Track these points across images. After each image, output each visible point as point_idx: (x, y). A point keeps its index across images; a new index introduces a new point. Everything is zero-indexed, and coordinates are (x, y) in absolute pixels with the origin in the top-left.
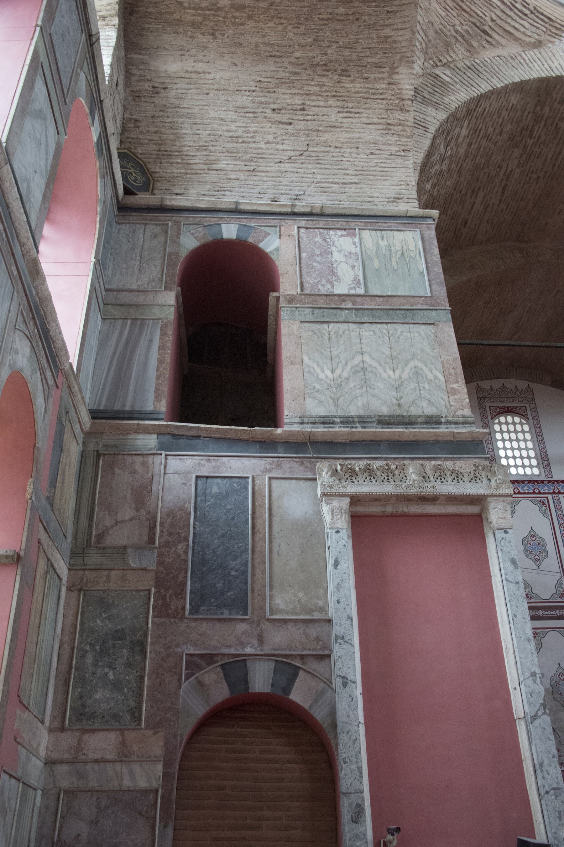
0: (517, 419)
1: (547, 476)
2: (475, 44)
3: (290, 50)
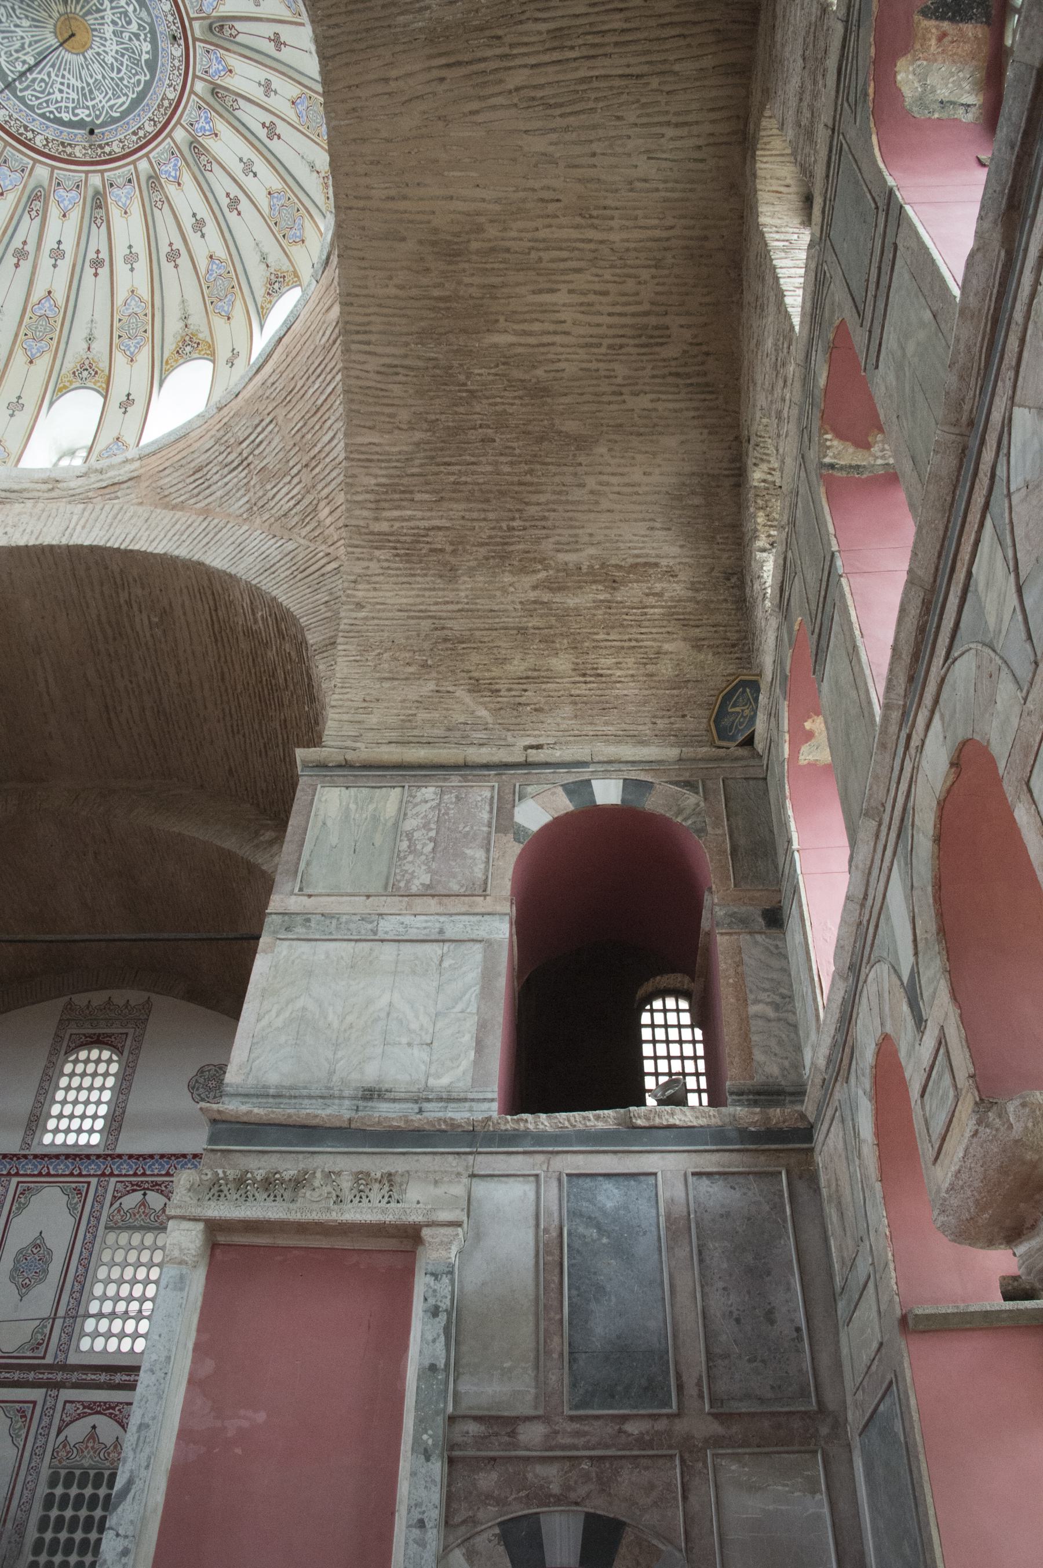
0: (106, 1054)
1: (106, 1147)
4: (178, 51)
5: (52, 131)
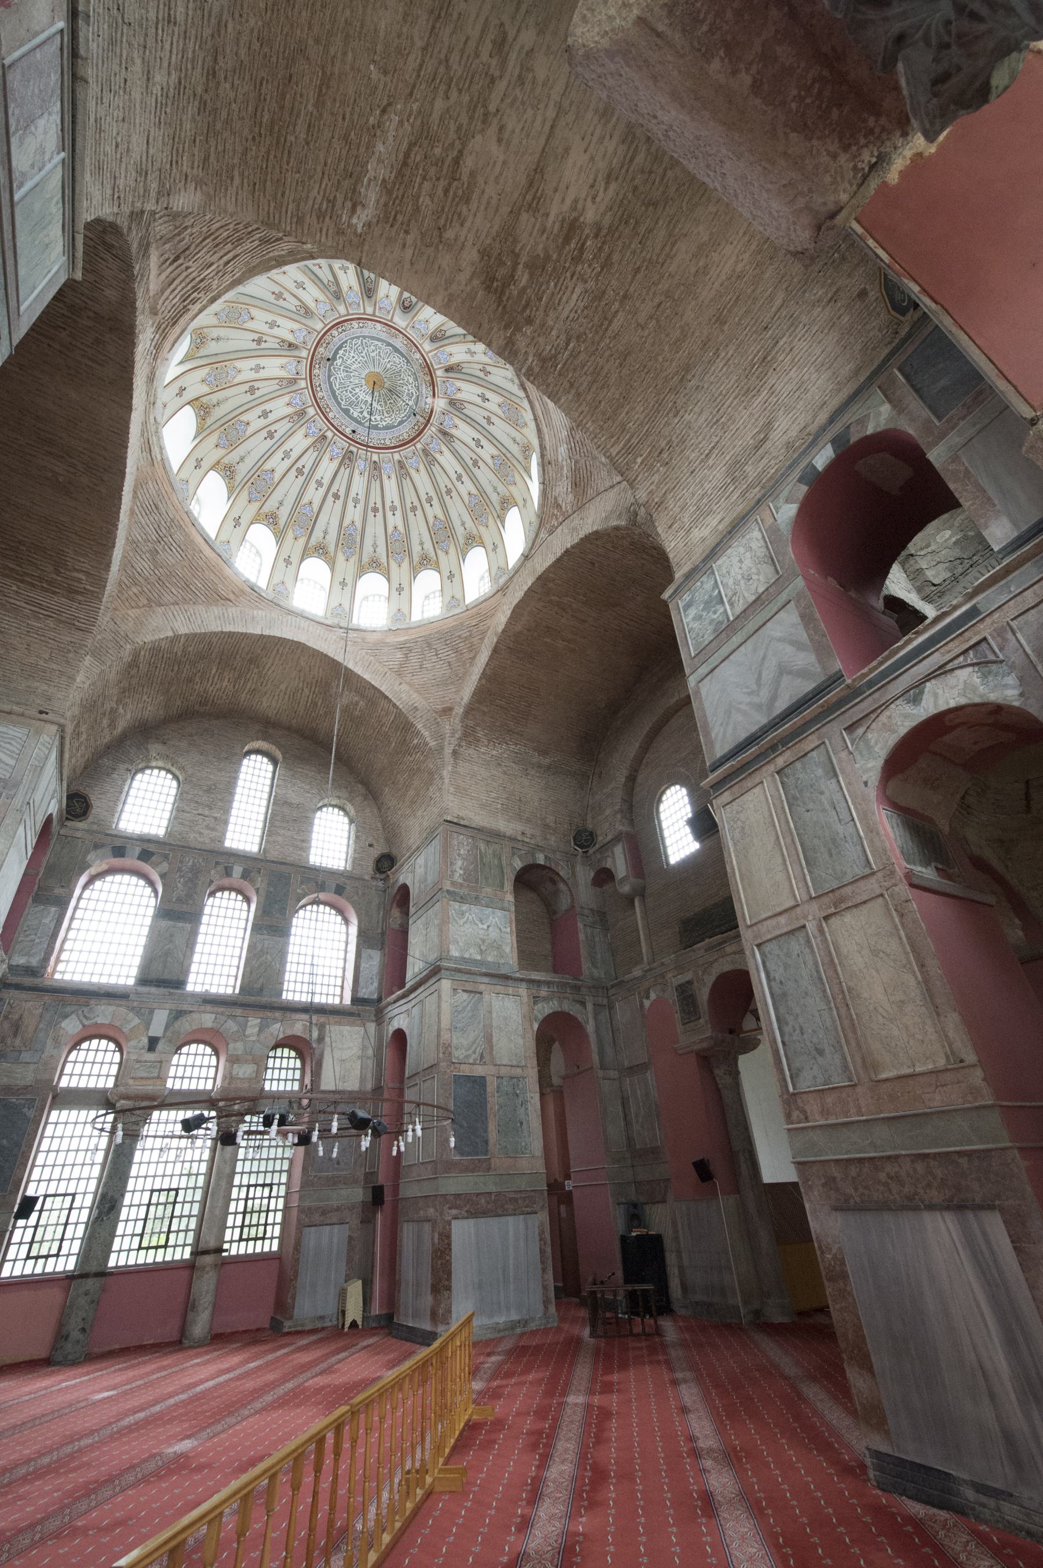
2: (167, 246)
3: (237, 16)
4: (348, 431)
5: (337, 341)
